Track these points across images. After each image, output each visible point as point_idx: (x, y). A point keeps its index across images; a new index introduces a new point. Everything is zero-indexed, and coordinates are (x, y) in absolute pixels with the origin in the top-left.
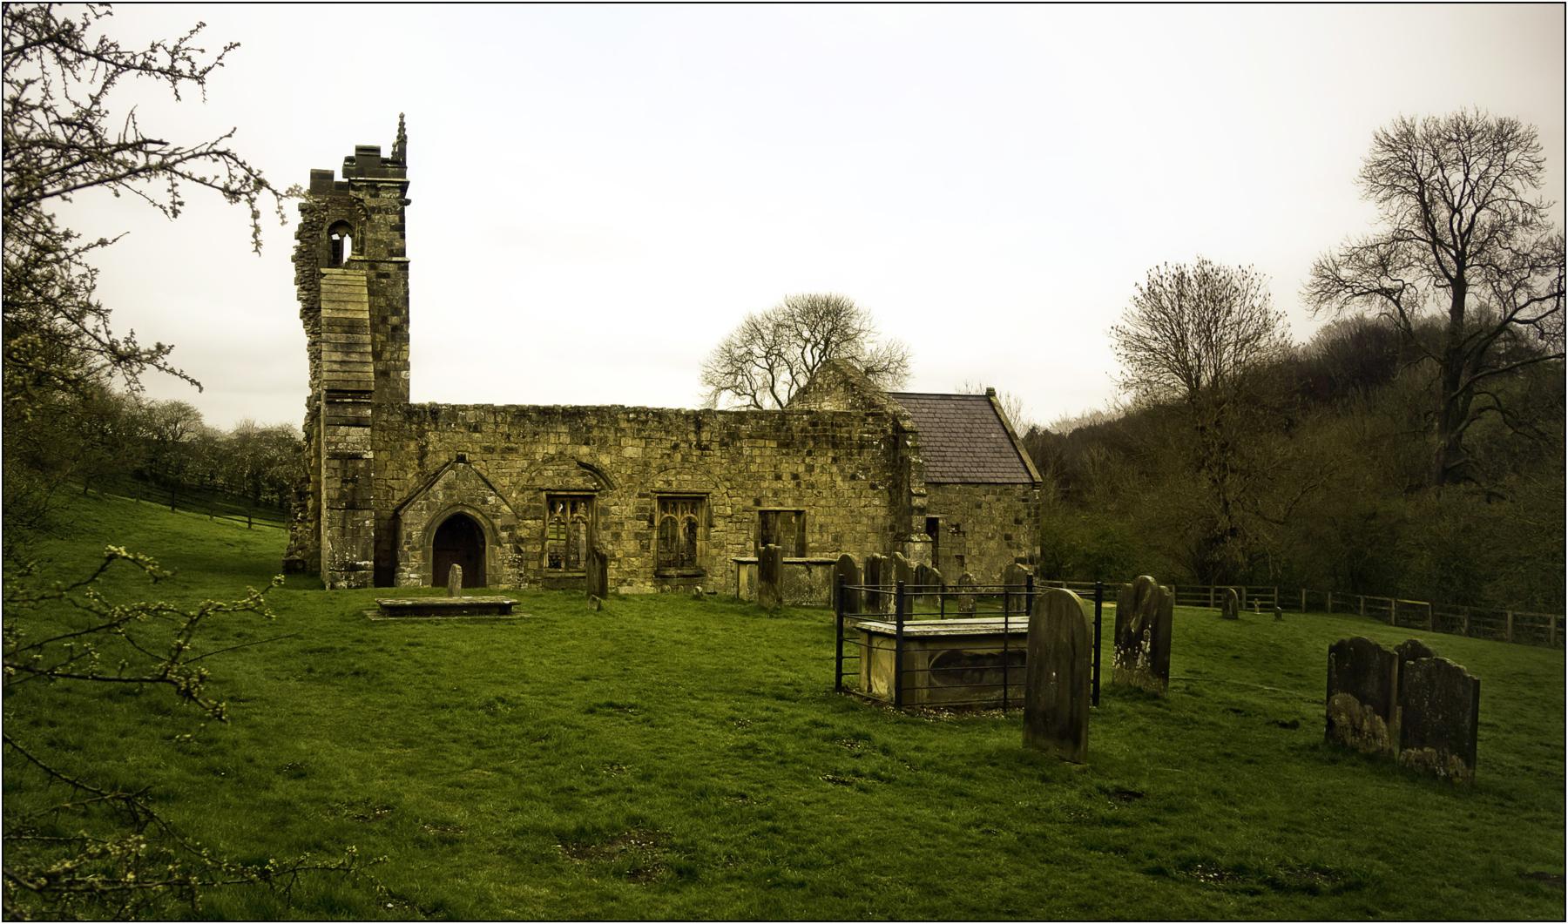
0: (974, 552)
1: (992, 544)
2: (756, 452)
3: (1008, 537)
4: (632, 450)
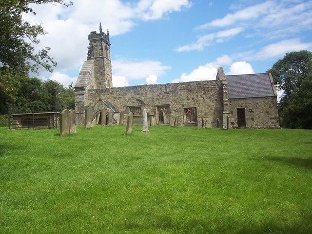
4: (149, 95)
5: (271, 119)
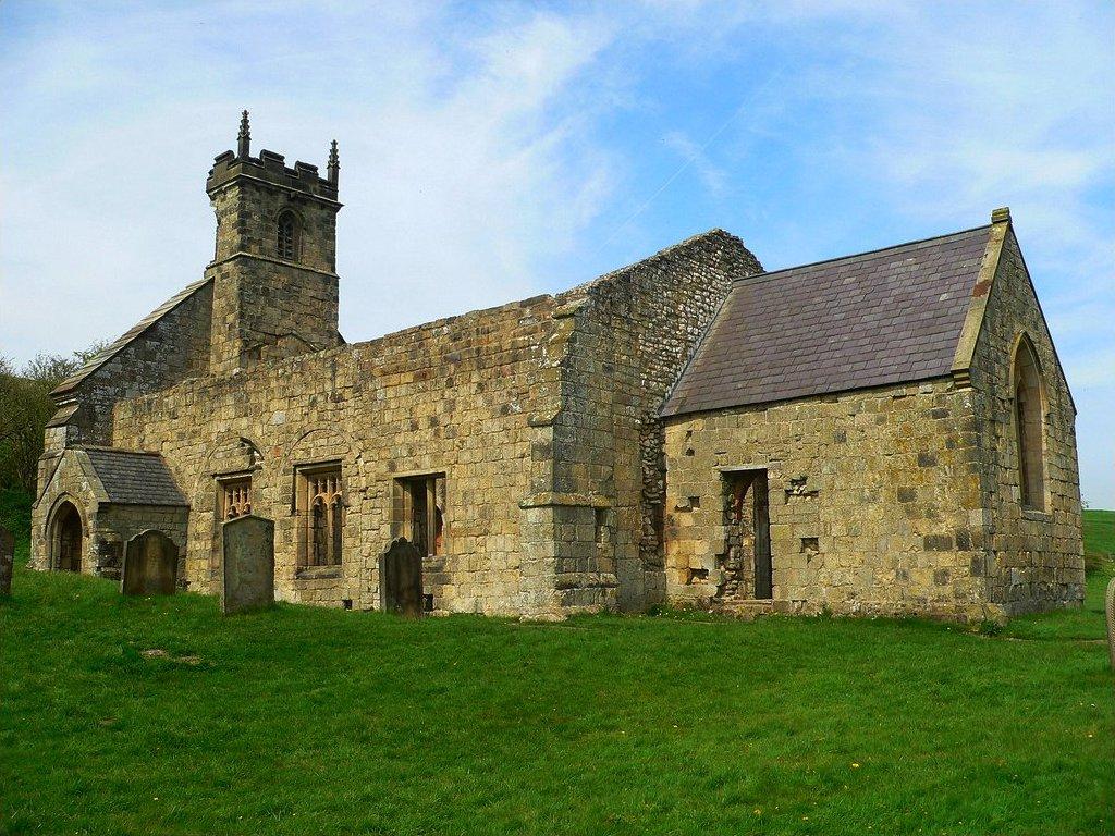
0: (836, 530)
1: (872, 510)
2: (391, 393)
3: (905, 496)
5: (932, 544)
